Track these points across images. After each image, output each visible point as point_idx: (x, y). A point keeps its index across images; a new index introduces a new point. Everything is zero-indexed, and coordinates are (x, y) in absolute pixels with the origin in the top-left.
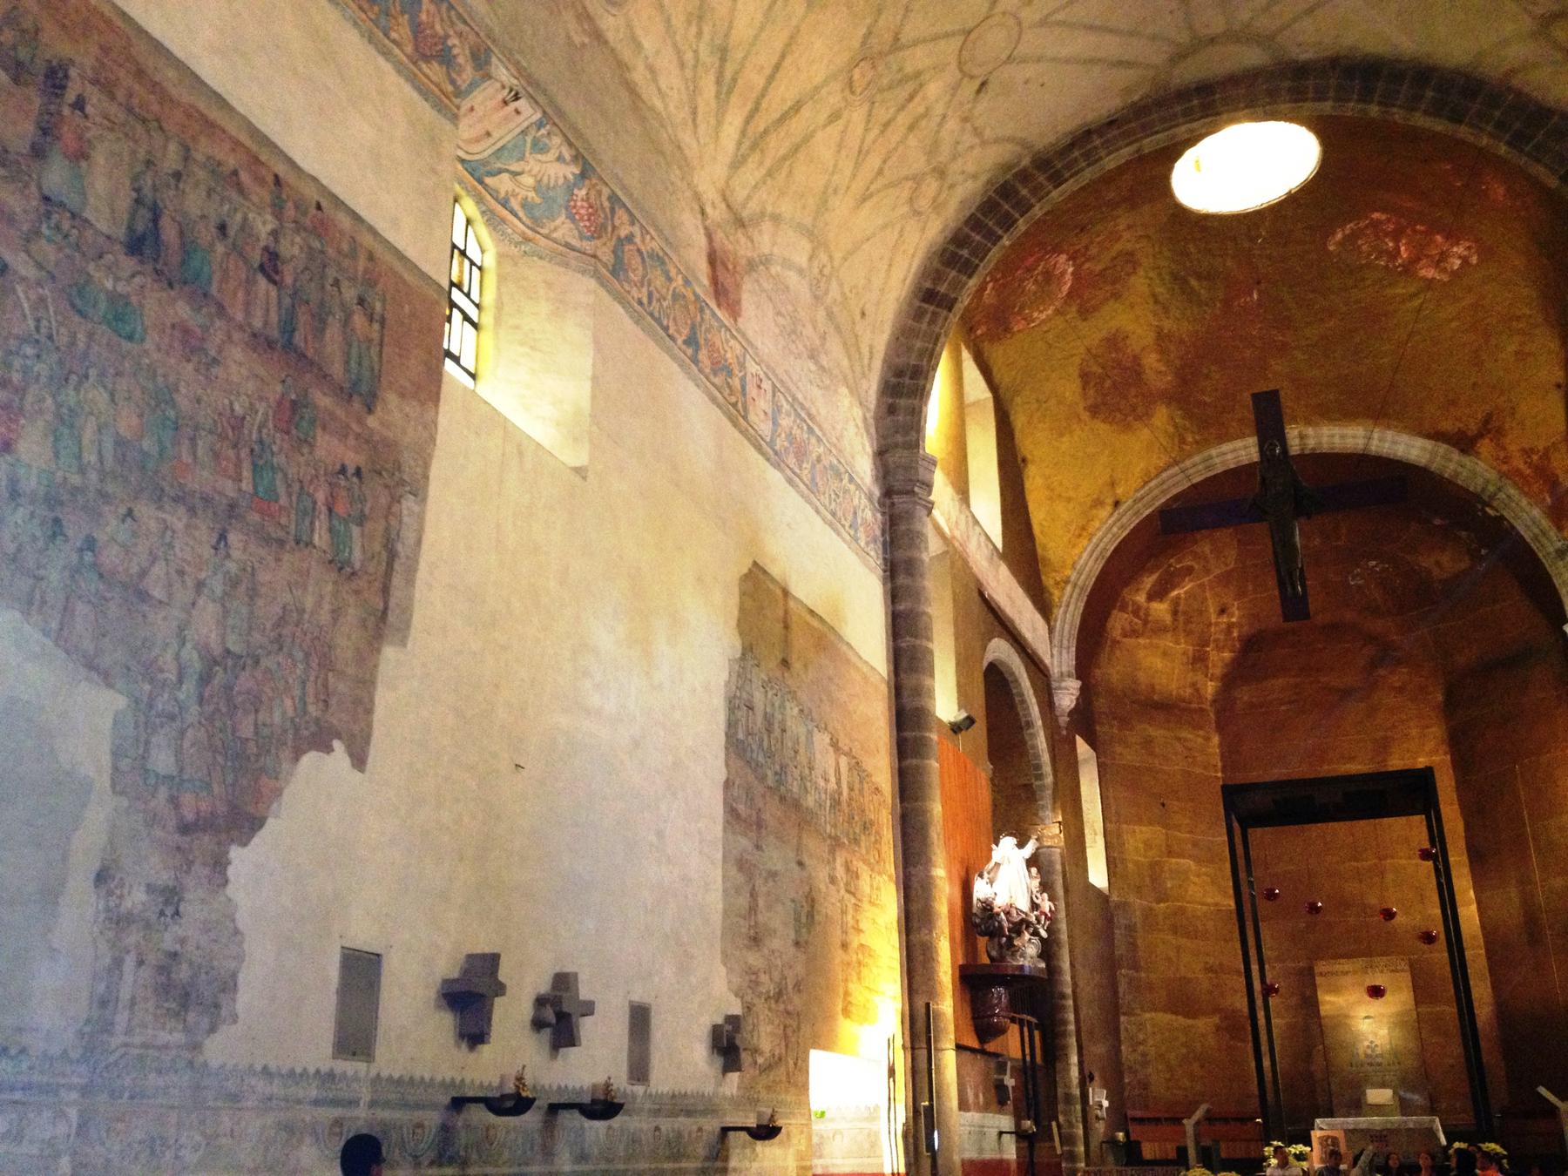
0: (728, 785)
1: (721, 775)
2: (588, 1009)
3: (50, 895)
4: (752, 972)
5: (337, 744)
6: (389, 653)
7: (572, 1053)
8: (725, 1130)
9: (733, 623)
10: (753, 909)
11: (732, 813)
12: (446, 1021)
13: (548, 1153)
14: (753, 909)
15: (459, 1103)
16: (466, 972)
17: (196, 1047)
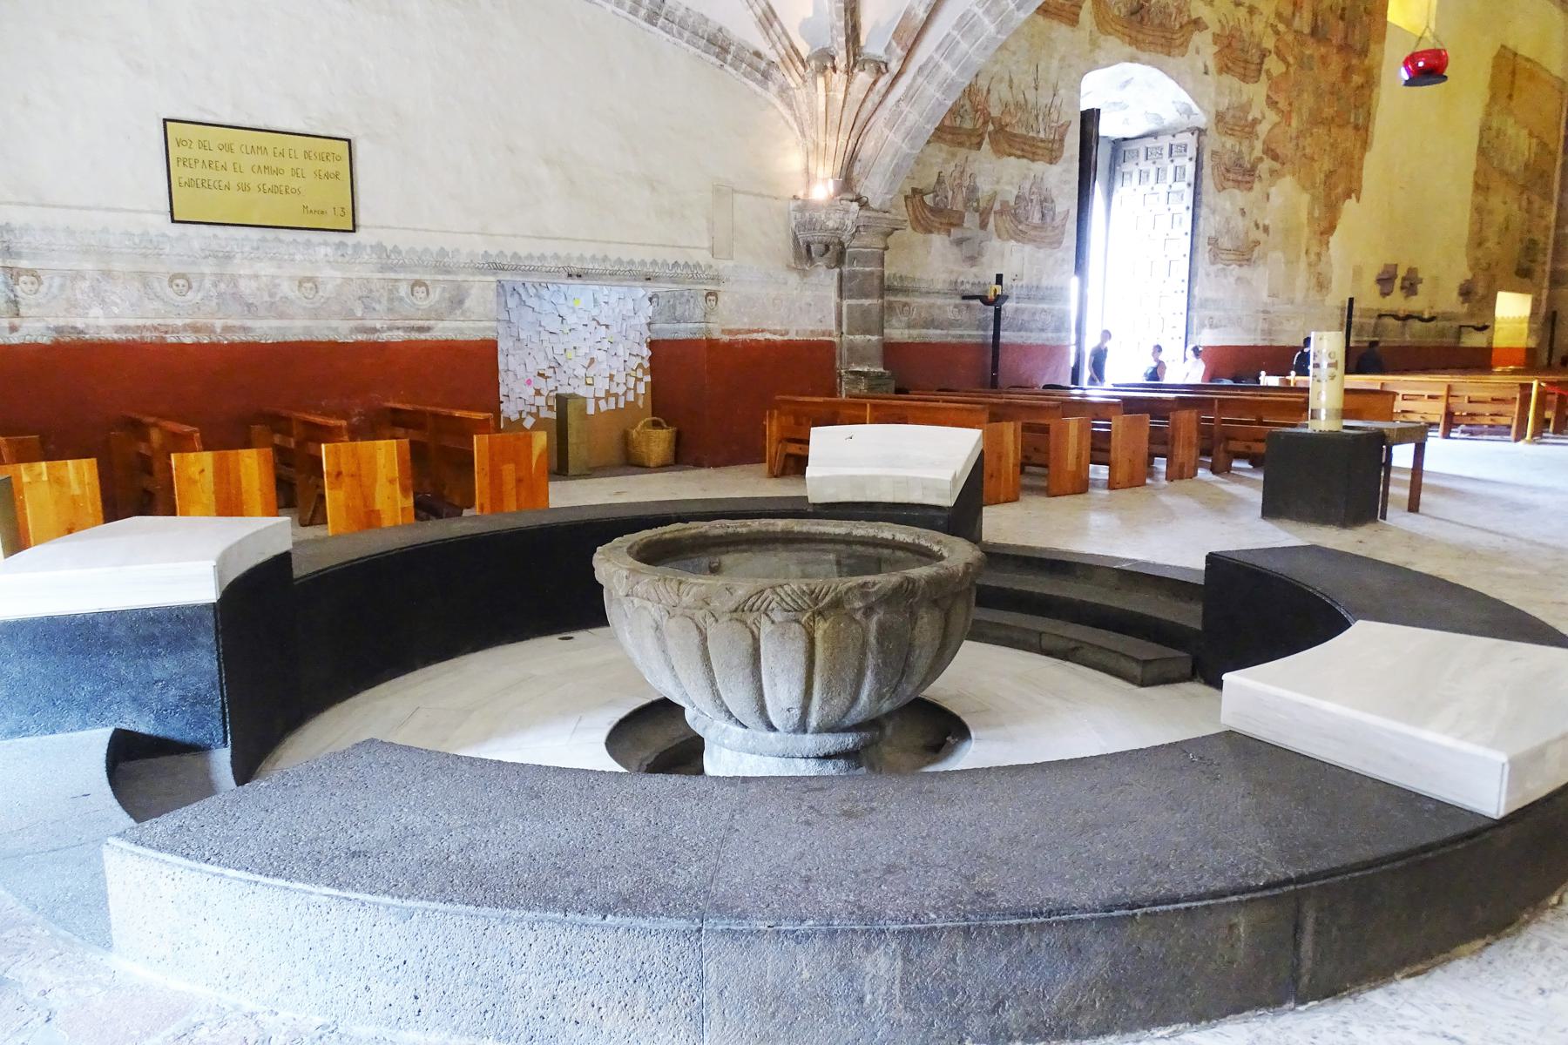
0: (1476, 173)
1: (1473, 167)
2: (1421, 281)
3: (1298, 257)
4: (1477, 259)
5: (1353, 195)
6: (1368, 156)
7: (1414, 298)
8: (1461, 326)
9: (1487, 84)
10: (1481, 229)
11: (1477, 186)
12: (1377, 288)
13: (1403, 334)
14: (1481, 229)
15: (1380, 316)
16: (1383, 273)
17: (1323, 301)
